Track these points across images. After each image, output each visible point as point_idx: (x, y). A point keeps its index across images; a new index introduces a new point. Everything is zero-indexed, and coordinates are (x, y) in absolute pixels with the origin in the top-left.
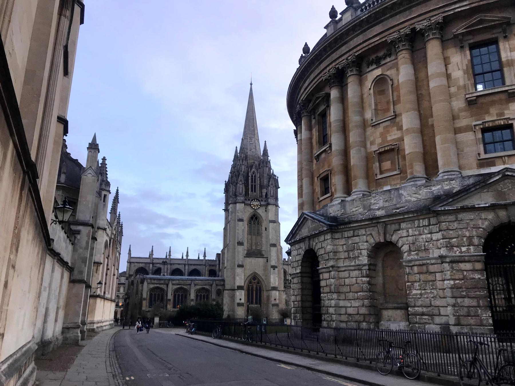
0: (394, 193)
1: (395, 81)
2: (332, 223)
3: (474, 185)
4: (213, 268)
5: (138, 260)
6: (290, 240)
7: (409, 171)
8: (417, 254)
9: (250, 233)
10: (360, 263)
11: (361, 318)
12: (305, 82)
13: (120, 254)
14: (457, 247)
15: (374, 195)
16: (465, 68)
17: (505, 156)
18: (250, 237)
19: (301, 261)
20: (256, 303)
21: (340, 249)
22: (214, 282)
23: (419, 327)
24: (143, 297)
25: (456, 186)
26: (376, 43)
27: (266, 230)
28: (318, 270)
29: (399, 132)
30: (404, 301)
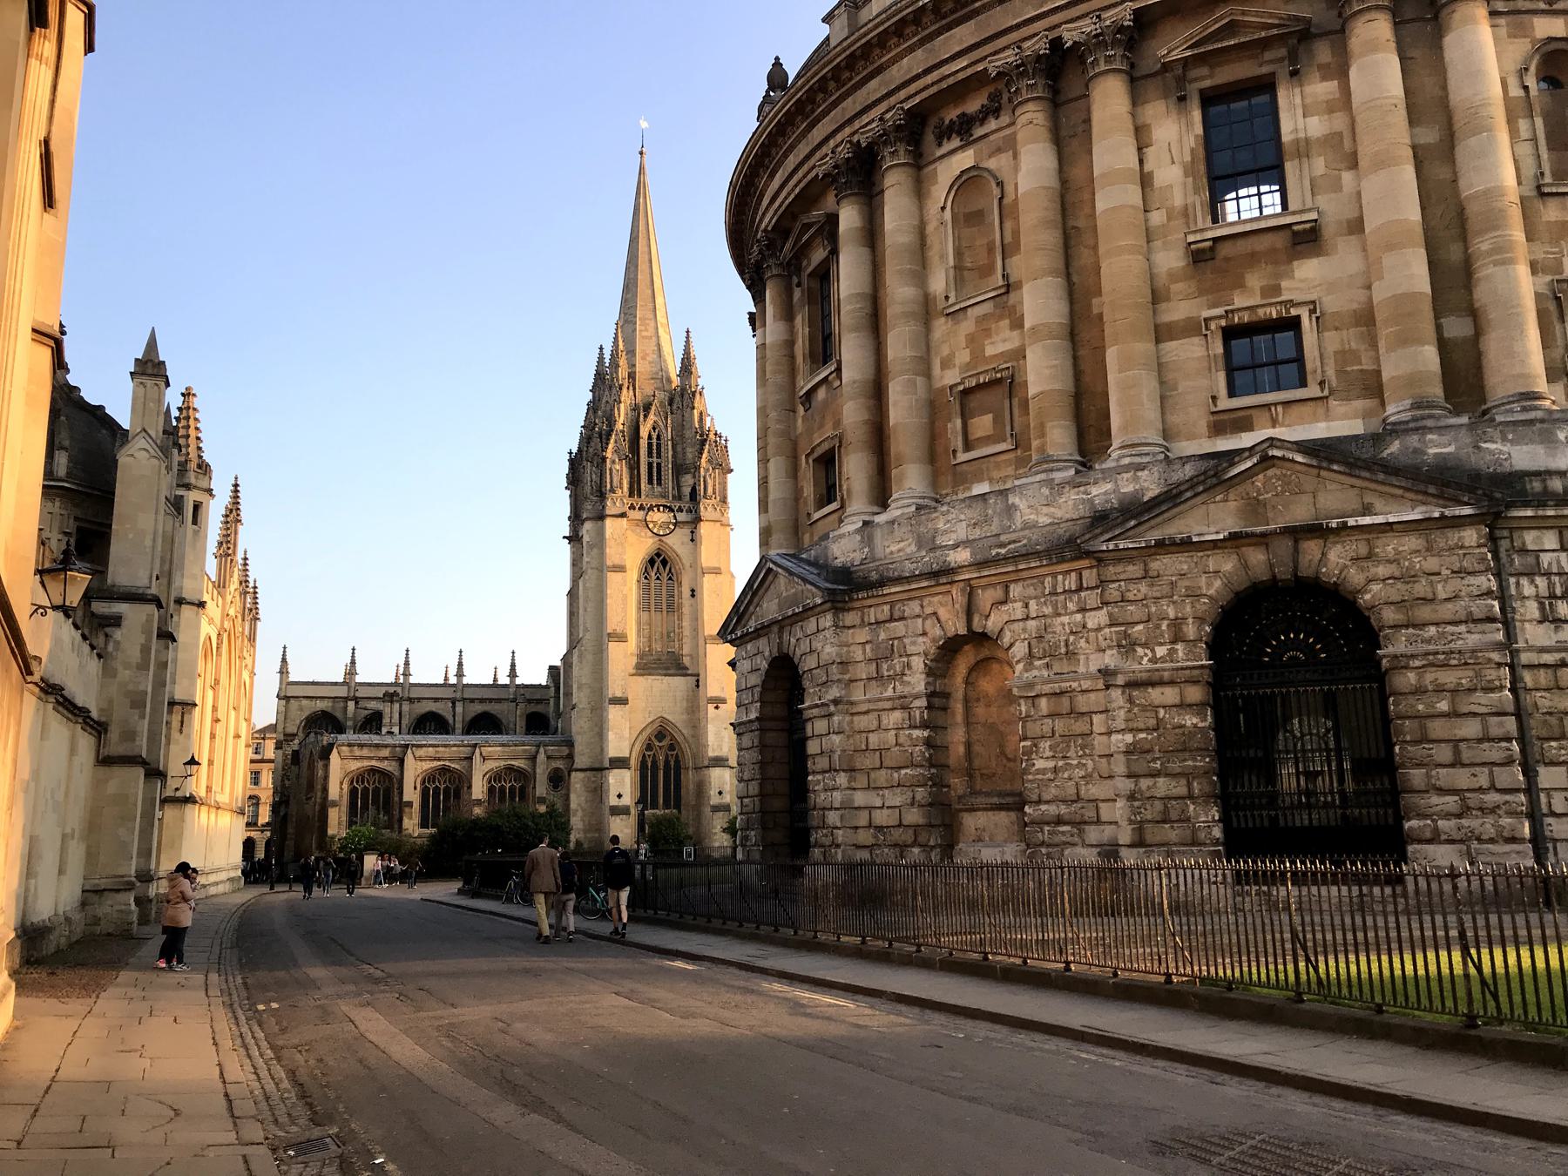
0: (995, 503)
1: (1009, 189)
2: (835, 586)
3: (1192, 483)
4: (539, 708)
5: (311, 691)
6: (731, 633)
7: (1035, 444)
8: (1048, 666)
9: (645, 605)
10: (907, 690)
11: (908, 837)
12: (772, 176)
13: (253, 674)
14: (1145, 645)
15: (945, 508)
16: (1188, 158)
17: (1276, 404)
18: (645, 615)
19: (759, 689)
20: (667, 805)
21: (858, 654)
22: (542, 750)
23: (1049, 856)
24: (331, 797)
25: (1150, 484)
26: (961, 76)
27: (693, 596)
28: (800, 712)
29: (1016, 333)
30: (1017, 787)
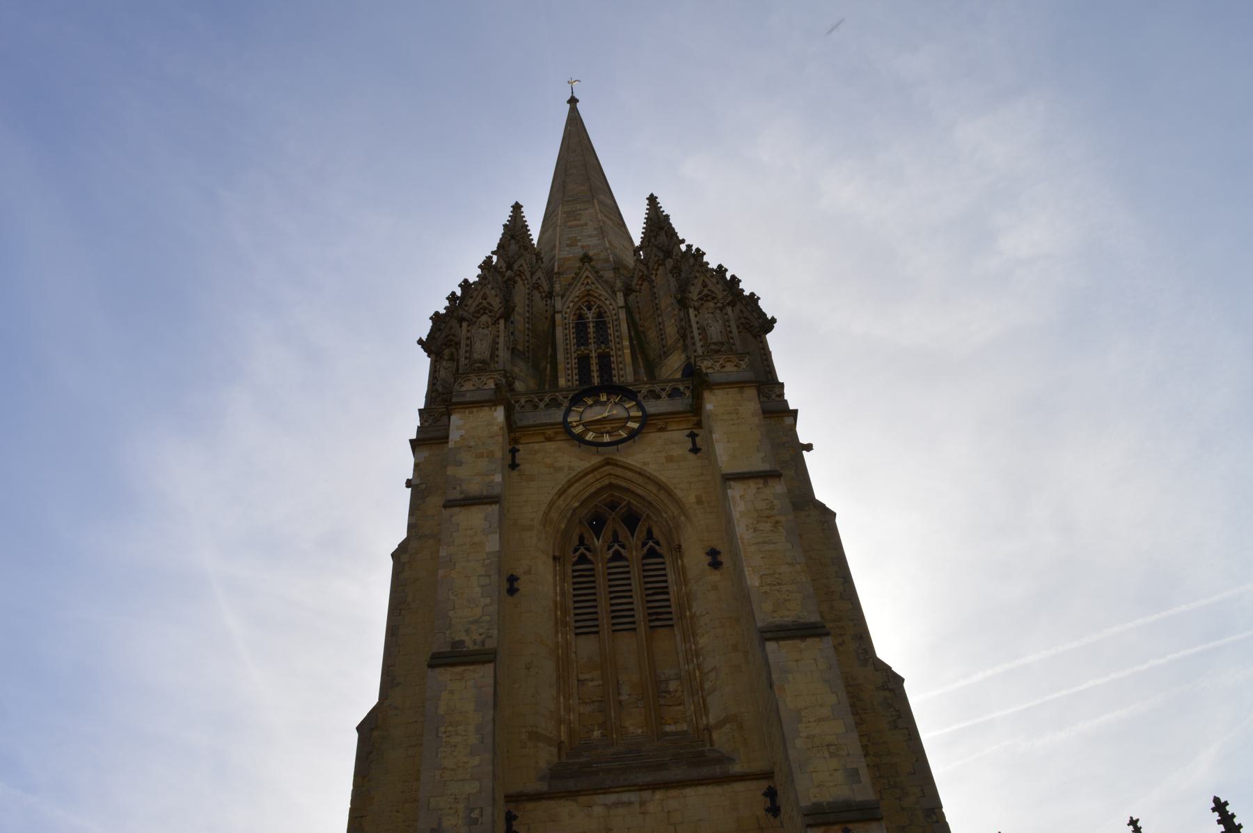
18: (586, 647)
27: (716, 564)
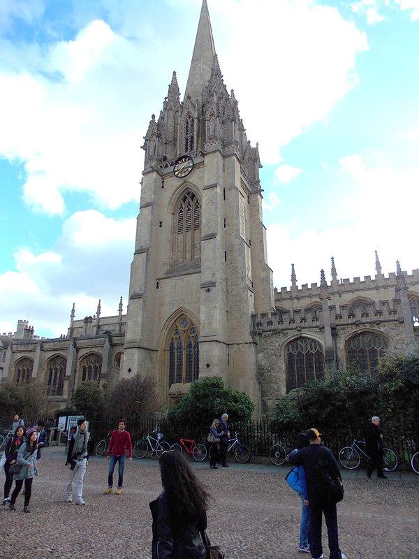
18: (181, 237)
20: (189, 380)
